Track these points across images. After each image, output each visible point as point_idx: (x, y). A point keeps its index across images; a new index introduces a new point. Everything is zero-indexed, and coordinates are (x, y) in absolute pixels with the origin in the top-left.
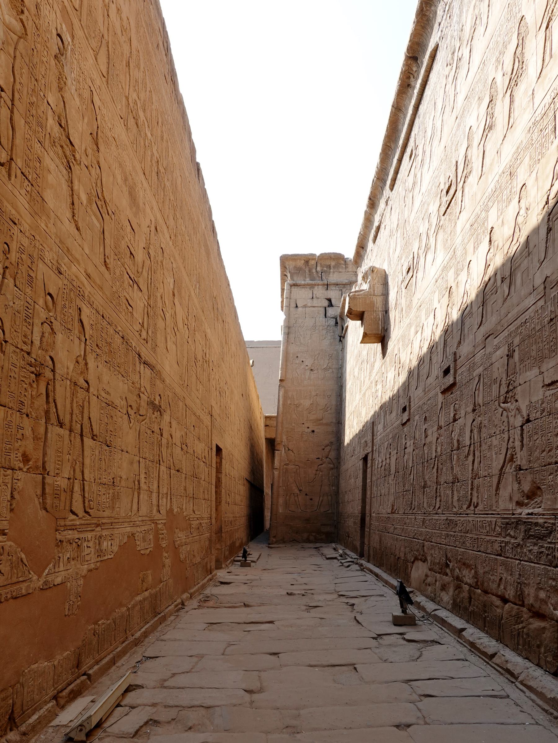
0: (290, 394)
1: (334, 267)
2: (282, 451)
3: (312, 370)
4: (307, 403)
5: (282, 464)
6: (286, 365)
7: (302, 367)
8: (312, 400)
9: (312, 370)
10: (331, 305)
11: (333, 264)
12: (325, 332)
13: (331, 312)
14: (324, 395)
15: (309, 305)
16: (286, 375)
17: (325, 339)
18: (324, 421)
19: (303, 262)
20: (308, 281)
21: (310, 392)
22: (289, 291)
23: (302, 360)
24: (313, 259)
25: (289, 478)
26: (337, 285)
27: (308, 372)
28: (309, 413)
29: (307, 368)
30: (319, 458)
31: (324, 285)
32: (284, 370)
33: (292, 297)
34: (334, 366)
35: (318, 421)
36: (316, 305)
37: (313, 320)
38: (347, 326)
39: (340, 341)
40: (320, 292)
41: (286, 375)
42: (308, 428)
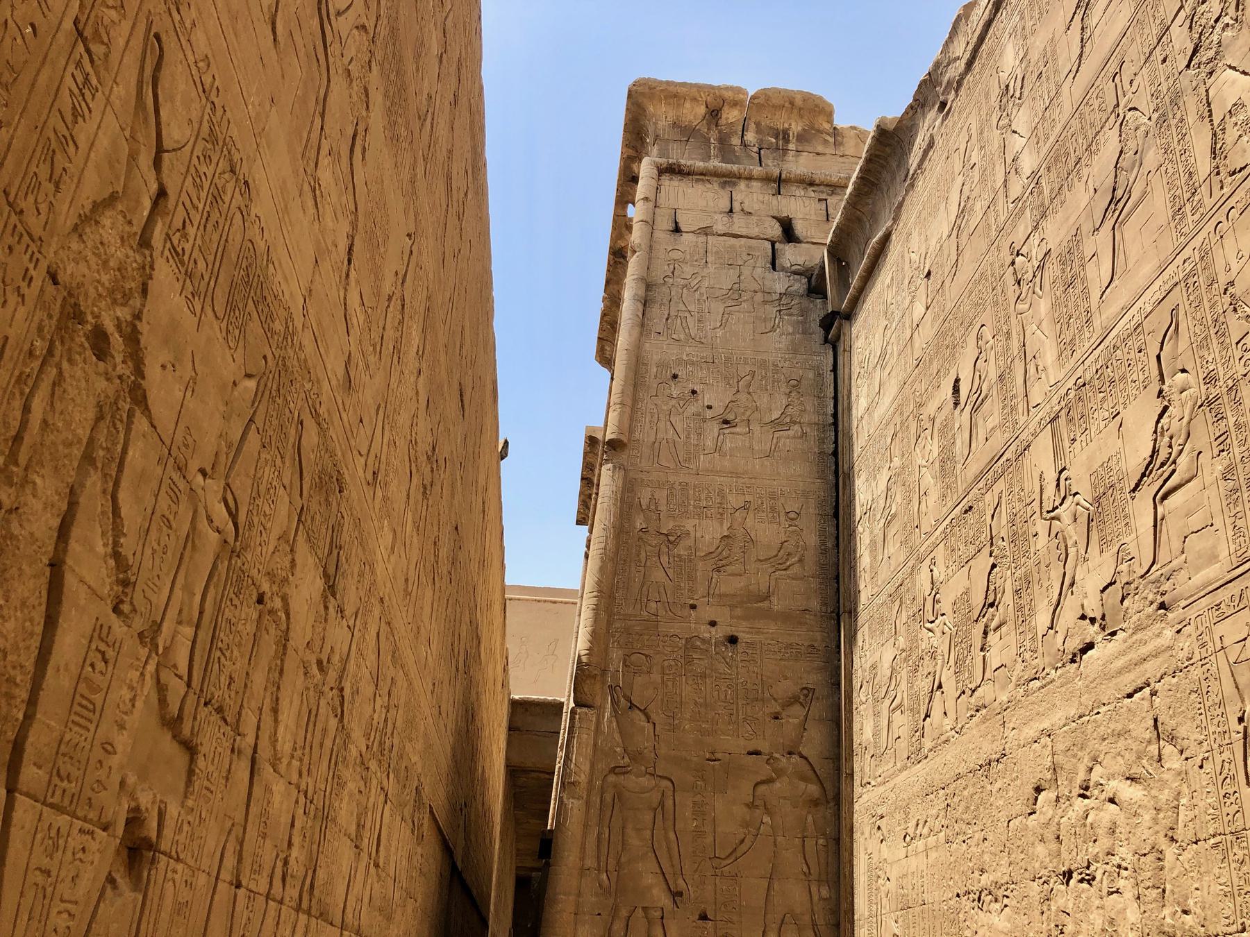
0: (645, 496)
1: (801, 138)
2: (601, 709)
3: (726, 422)
4: (708, 532)
5: (602, 766)
6: (635, 400)
7: (693, 409)
8: (726, 525)
9: (726, 422)
10: (789, 233)
11: (796, 127)
12: (772, 310)
13: (791, 255)
14: (773, 509)
15: (720, 228)
16: (631, 431)
17: (773, 329)
18: (777, 604)
19: (702, 110)
20: (715, 163)
21: (721, 494)
22: (654, 183)
23: (691, 386)
24: (735, 104)
25: (630, 831)
26: (811, 184)
27: (713, 429)
28: (718, 569)
29: (709, 414)
30: (757, 753)
31: (767, 179)
32: (628, 410)
33: (661, 201)
34: (806, 418)
35: (754, 603)
36: (743, 232)
37: (733, 273)
38: (887, 238)
39: (826, 341)
40: (752, 196)
41: (631, 431)
42: (713, 624)
